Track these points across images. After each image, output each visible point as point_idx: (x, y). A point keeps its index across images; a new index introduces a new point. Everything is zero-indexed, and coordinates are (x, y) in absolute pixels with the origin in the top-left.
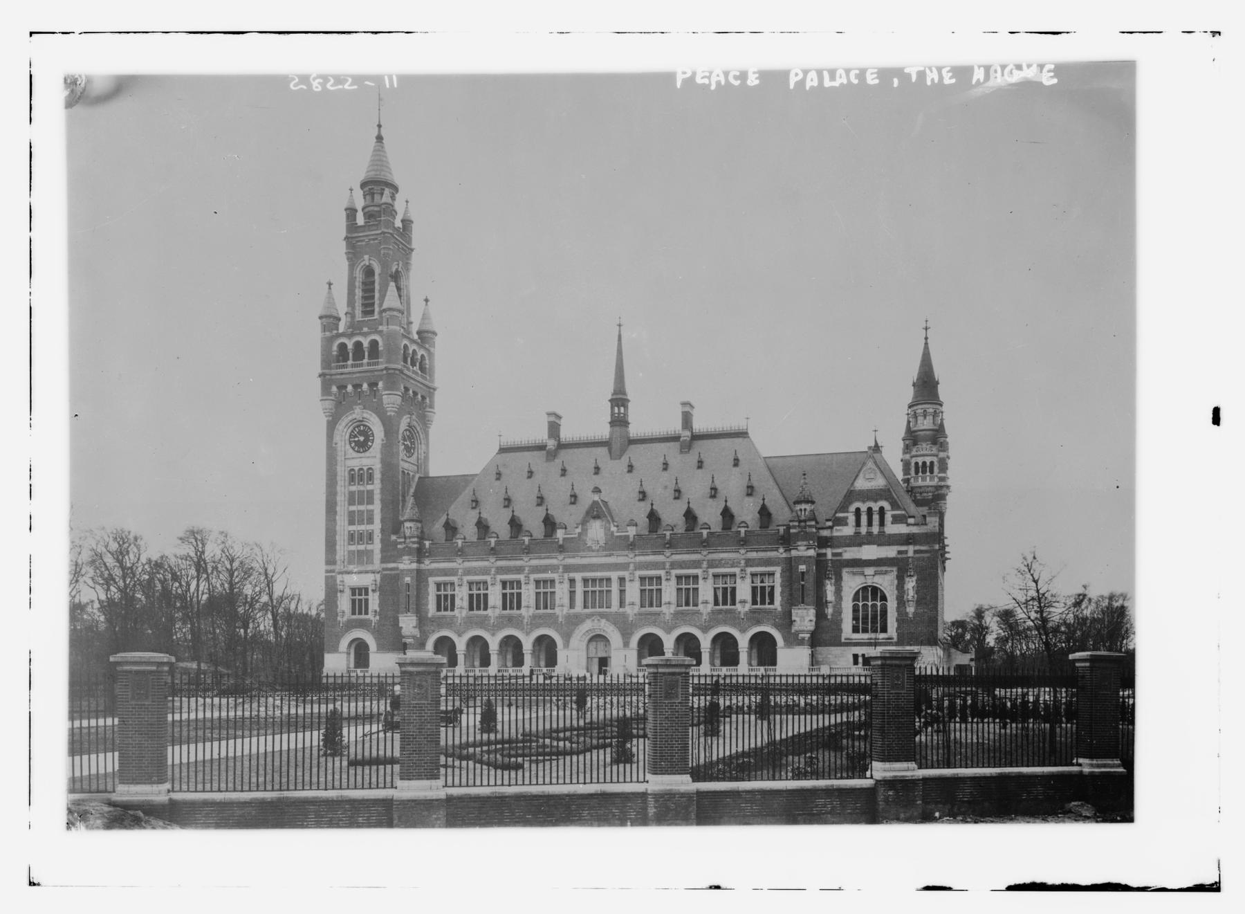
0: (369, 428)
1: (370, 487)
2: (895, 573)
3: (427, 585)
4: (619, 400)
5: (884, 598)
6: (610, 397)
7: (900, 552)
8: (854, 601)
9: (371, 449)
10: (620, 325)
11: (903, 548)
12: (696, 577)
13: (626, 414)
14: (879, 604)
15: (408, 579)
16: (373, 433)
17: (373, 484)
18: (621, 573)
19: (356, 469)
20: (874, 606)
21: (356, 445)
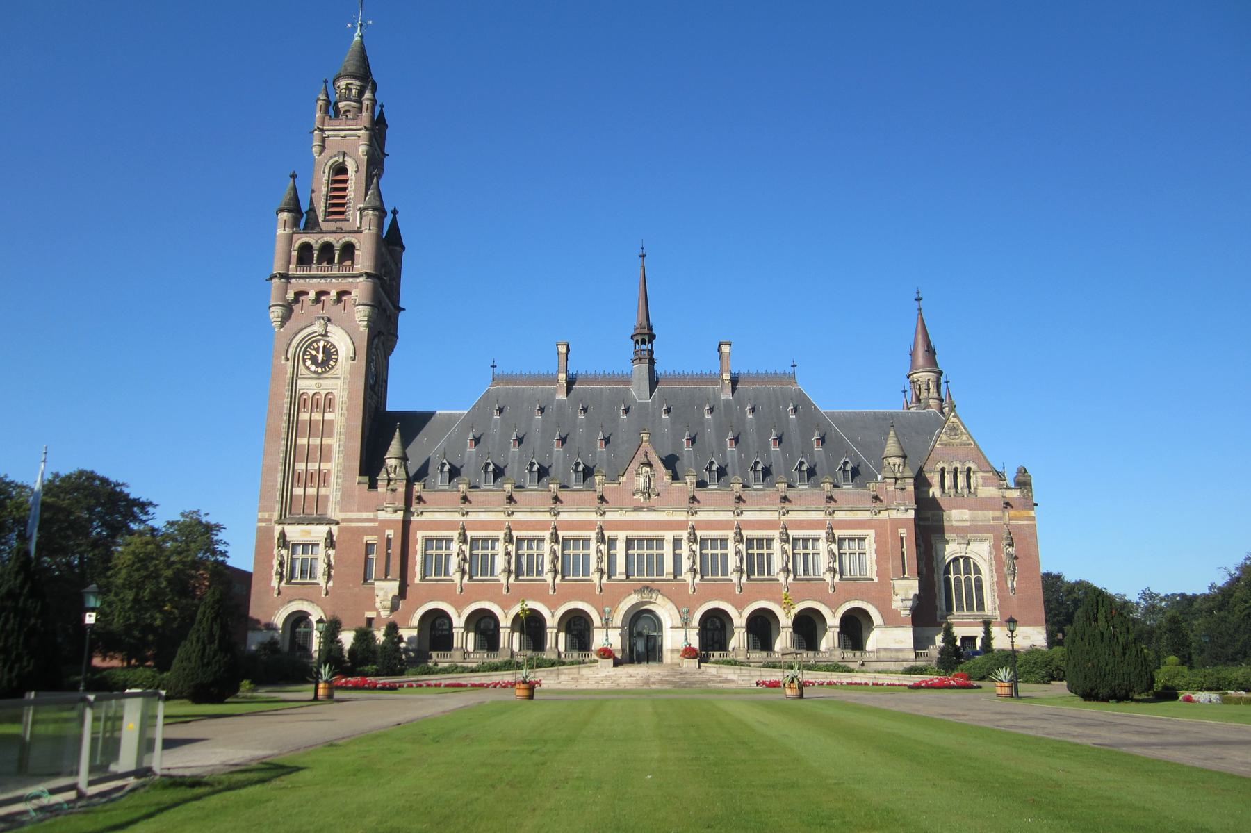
0: (332, 344)
1: (328, 416)
2: (992, 544)
3: (417, 540)
4: (646, 336)
5: (977, 571)
6: (632, 332)
7: (994, 519)
8: (944, 575)
9: (332, 372)
10: (643, 256)
11: (998, 513)
12: (770, 540)
13: (651, 352)
14: (973, 577)
15: (390, 533)
16: (337, 351)
17: (333, 411)
18: (677, 533)
19: (311, 393)
20: (968, 580)
21: (312, 364)
